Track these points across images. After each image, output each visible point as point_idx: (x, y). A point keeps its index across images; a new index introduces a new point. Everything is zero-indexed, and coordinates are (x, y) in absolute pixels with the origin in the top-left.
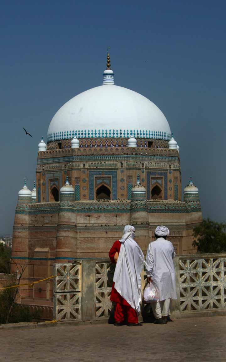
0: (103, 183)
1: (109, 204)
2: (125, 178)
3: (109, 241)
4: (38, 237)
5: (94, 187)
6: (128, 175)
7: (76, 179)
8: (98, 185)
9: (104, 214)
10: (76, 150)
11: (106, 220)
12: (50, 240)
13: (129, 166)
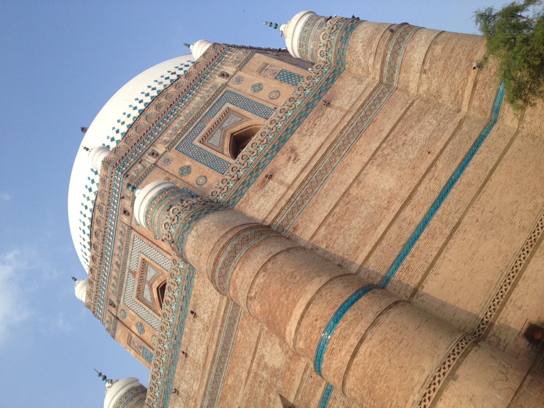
5: (219, 155)
11: (319, 135)
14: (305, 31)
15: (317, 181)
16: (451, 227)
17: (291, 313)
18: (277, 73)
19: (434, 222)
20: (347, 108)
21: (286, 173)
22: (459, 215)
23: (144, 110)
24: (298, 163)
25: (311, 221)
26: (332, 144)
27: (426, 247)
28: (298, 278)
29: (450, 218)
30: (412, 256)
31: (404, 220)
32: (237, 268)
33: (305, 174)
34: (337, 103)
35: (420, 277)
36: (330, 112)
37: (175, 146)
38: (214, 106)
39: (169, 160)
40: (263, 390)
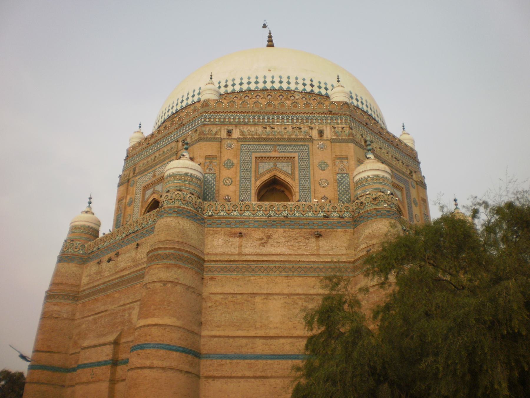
0: (274, 172)
1: (295, 207)
2: (329, 162)
3: (297, 304)
4: (97, 310)
5: (253, 179)
6: (338, 153)
7: (207, 161)
8: (263, 174)
9: (281, 231)
10: (212, 103)
12: (124, 310)
13: (337, 136)
14: (367, 181)
15: (253, 270)
16: (263, 374)
17: (147, 318)
18: (343, 172)
19: (261, 363)
20: (321, 252)
21: (249, 245)
22: (274, 374)
23: (268, 90)
24: (261, 247)
25: (223, 286)
26: (286, 261)
27: (242, 367)
28: (170, 307)
29: (269, 371)
30: (231, 363)
31: (254, 343)
32: (158, 266)
33: (255, 258)
34: (322, 242)
35: (219, 375)
36: (312, 242)
37: (243, 143)
38: (290, 145)
39: (230, 146)
40: (120, 320)
